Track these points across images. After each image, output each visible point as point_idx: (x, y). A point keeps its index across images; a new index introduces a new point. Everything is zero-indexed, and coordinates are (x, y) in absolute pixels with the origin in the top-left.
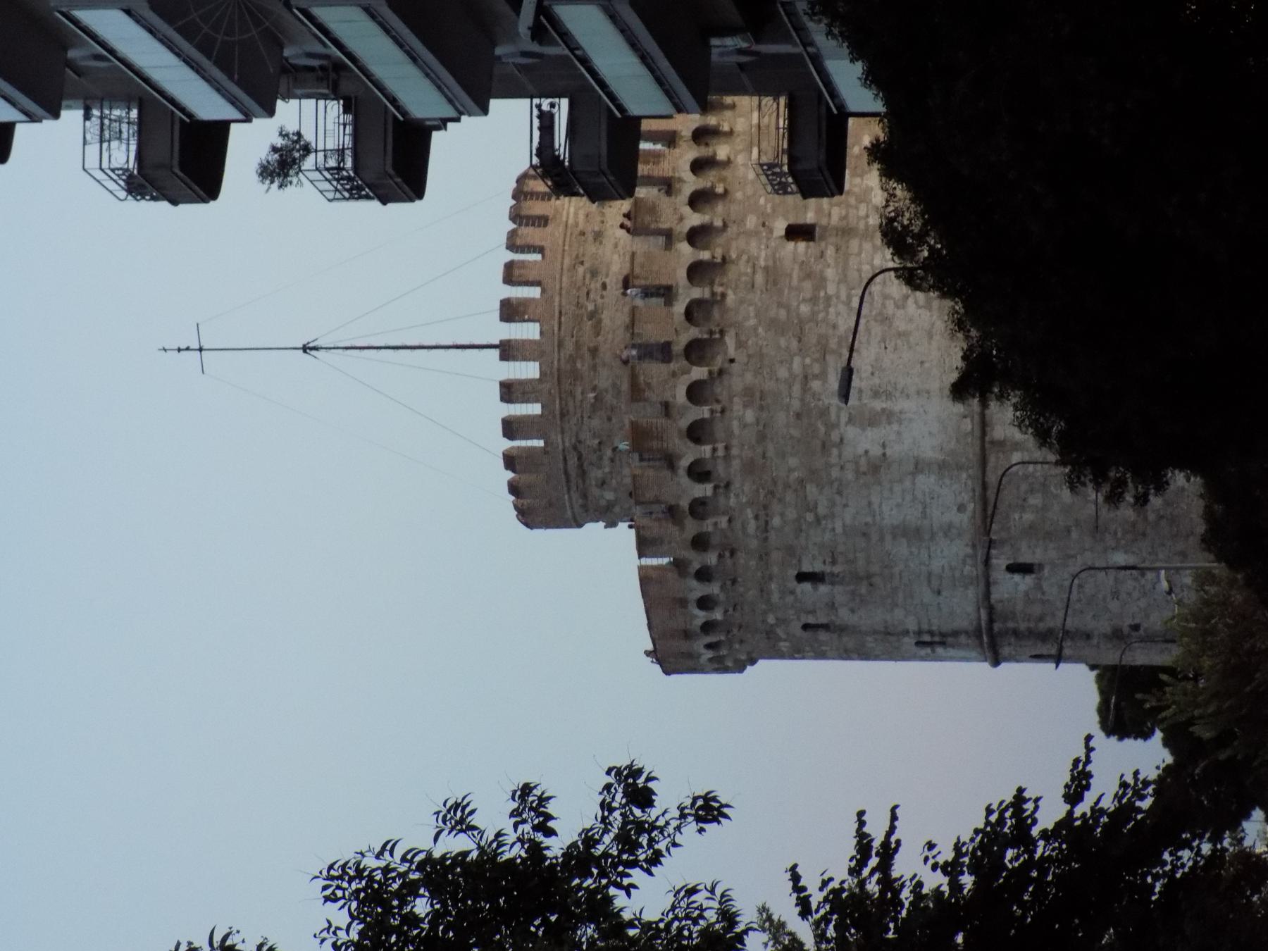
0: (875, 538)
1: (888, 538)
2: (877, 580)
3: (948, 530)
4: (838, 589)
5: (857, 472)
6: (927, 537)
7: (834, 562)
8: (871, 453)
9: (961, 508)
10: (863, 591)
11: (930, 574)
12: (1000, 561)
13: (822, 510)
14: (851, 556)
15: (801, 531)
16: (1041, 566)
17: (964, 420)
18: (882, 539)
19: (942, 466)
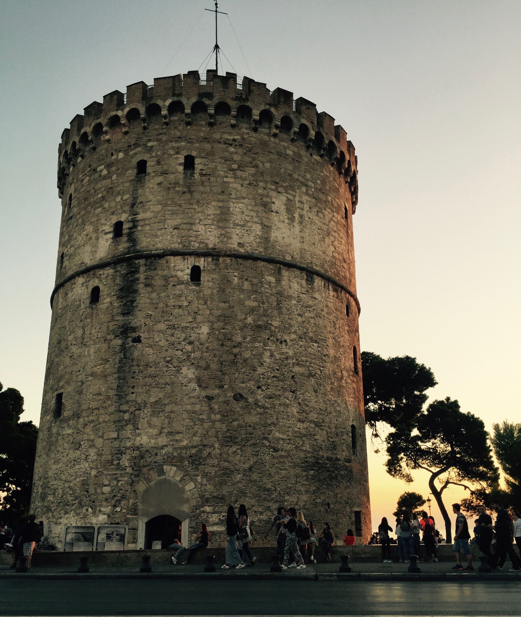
0: (221, 197)
1: (221, 204)
2: (188, 196)
3: (227, 236)
4: (181, 176)
5: (262, 195)
6: (220, 224)
7: (201, 175)
8: (273, 205)
9: (240, 244)
10: (178, 189)
11: (192, 224)
12: (201, 262)
13: (239, 173)
14: (206, 184)
15: (226, 161)
16: (198, 285)
17: (291, 257)
18: (219, 201)
19: (267, 239)
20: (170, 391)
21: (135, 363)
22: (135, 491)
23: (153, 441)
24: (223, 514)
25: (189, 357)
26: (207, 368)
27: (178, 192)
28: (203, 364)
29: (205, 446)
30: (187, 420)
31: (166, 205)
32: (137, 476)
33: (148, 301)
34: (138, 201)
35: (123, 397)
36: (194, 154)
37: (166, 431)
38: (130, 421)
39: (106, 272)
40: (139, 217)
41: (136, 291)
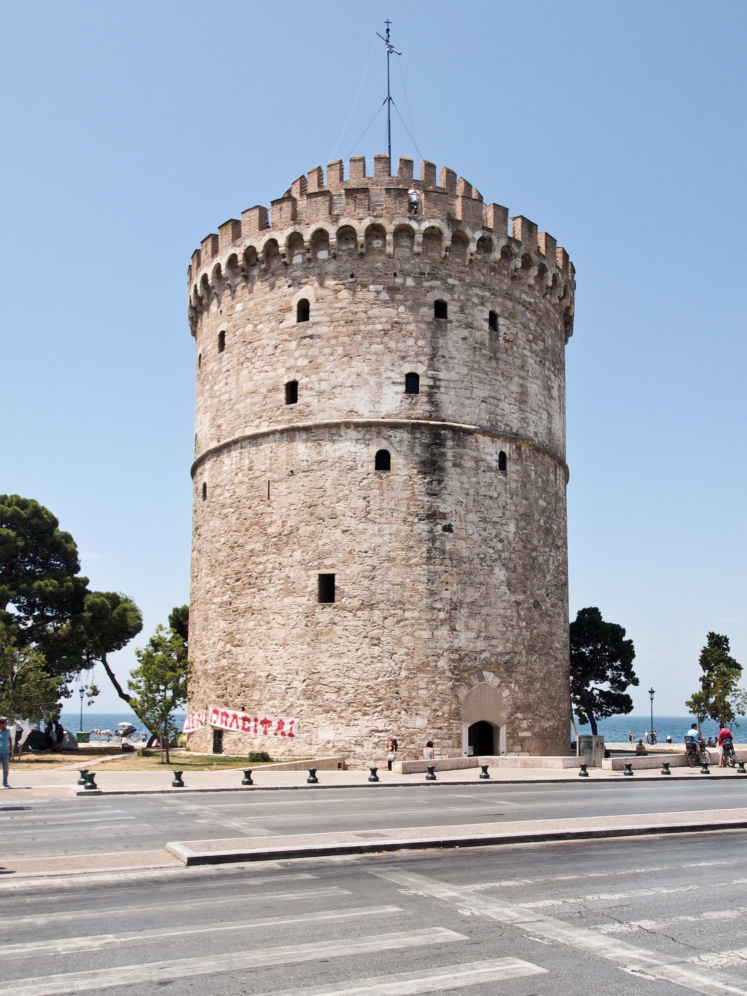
2: (494, 364)
4: (487, 336)
10: (484, 351)
20: (485, 592)
21: (447, 556)
22: (457, 696)
23: (472, 645)
24: (530, 720)
25: (500, 556)
26: (515, 570)
27: (484, 355)
28: (511, 565)
29: (515, 653)
30: (501, 625)
31: (472, 369)
32: (456, 680)
33: (459, 484)
34: (439, 354)
35: (436, 593)
36: (498, 311)
37: (483, 635)
38: (446, 620)
39: (398, 435)
40: (442, 375)
41: (442, 469)
